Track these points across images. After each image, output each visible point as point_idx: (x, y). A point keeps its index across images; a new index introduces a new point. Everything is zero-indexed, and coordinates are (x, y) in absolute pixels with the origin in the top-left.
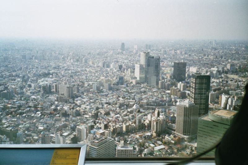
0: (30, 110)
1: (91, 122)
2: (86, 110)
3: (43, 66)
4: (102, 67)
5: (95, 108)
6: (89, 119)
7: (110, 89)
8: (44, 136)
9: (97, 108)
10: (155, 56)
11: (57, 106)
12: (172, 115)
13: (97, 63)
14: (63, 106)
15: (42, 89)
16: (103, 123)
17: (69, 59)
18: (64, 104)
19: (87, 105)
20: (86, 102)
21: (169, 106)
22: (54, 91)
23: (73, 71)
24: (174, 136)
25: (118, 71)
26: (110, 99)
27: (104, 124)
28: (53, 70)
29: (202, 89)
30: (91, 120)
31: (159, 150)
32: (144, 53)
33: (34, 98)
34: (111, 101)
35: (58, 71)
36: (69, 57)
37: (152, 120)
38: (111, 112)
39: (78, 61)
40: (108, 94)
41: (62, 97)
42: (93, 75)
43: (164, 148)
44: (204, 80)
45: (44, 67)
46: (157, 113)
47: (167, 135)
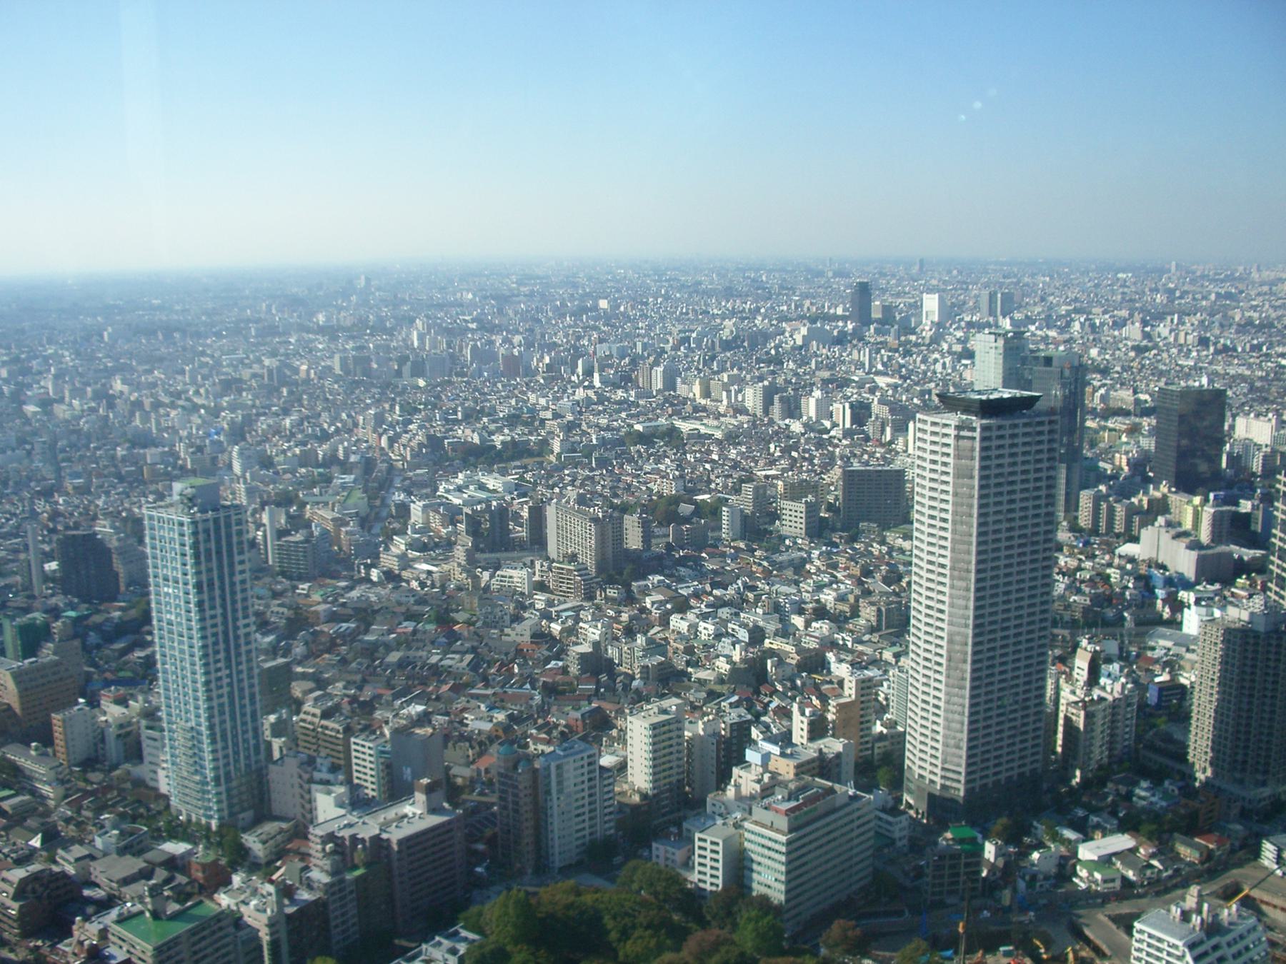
0: (415, 632)
3: (455, 413)
4: (759, 413)
5: (743, 635)
6: (718, 688)
7: (817, 530)
8: (511, 764)
12: (1165, 677)
13: (729, 392)
15: (462, 527)
16: (803, 714)
17: (580, 370)
18: (581, 608)
19: (704, 617)
20: (693, 602)
21: (1142, 629)
23: (608, 435)
24: (1180, 789)
25: (847, 434)
26: (819, 588)
27: (805, 720)
28: (506, 431)
30: (733, 693)
31: (1106, 861)
33: (429, 573)
35: (531, 433)
36: (580, 362)
37: (1062, 701)
38: (831, 656)
39: (625, 380)
40: (804, 561)
43: (1133, 851)
45: (460, 416)
46: (1085, 666)
47: (1144, 784)
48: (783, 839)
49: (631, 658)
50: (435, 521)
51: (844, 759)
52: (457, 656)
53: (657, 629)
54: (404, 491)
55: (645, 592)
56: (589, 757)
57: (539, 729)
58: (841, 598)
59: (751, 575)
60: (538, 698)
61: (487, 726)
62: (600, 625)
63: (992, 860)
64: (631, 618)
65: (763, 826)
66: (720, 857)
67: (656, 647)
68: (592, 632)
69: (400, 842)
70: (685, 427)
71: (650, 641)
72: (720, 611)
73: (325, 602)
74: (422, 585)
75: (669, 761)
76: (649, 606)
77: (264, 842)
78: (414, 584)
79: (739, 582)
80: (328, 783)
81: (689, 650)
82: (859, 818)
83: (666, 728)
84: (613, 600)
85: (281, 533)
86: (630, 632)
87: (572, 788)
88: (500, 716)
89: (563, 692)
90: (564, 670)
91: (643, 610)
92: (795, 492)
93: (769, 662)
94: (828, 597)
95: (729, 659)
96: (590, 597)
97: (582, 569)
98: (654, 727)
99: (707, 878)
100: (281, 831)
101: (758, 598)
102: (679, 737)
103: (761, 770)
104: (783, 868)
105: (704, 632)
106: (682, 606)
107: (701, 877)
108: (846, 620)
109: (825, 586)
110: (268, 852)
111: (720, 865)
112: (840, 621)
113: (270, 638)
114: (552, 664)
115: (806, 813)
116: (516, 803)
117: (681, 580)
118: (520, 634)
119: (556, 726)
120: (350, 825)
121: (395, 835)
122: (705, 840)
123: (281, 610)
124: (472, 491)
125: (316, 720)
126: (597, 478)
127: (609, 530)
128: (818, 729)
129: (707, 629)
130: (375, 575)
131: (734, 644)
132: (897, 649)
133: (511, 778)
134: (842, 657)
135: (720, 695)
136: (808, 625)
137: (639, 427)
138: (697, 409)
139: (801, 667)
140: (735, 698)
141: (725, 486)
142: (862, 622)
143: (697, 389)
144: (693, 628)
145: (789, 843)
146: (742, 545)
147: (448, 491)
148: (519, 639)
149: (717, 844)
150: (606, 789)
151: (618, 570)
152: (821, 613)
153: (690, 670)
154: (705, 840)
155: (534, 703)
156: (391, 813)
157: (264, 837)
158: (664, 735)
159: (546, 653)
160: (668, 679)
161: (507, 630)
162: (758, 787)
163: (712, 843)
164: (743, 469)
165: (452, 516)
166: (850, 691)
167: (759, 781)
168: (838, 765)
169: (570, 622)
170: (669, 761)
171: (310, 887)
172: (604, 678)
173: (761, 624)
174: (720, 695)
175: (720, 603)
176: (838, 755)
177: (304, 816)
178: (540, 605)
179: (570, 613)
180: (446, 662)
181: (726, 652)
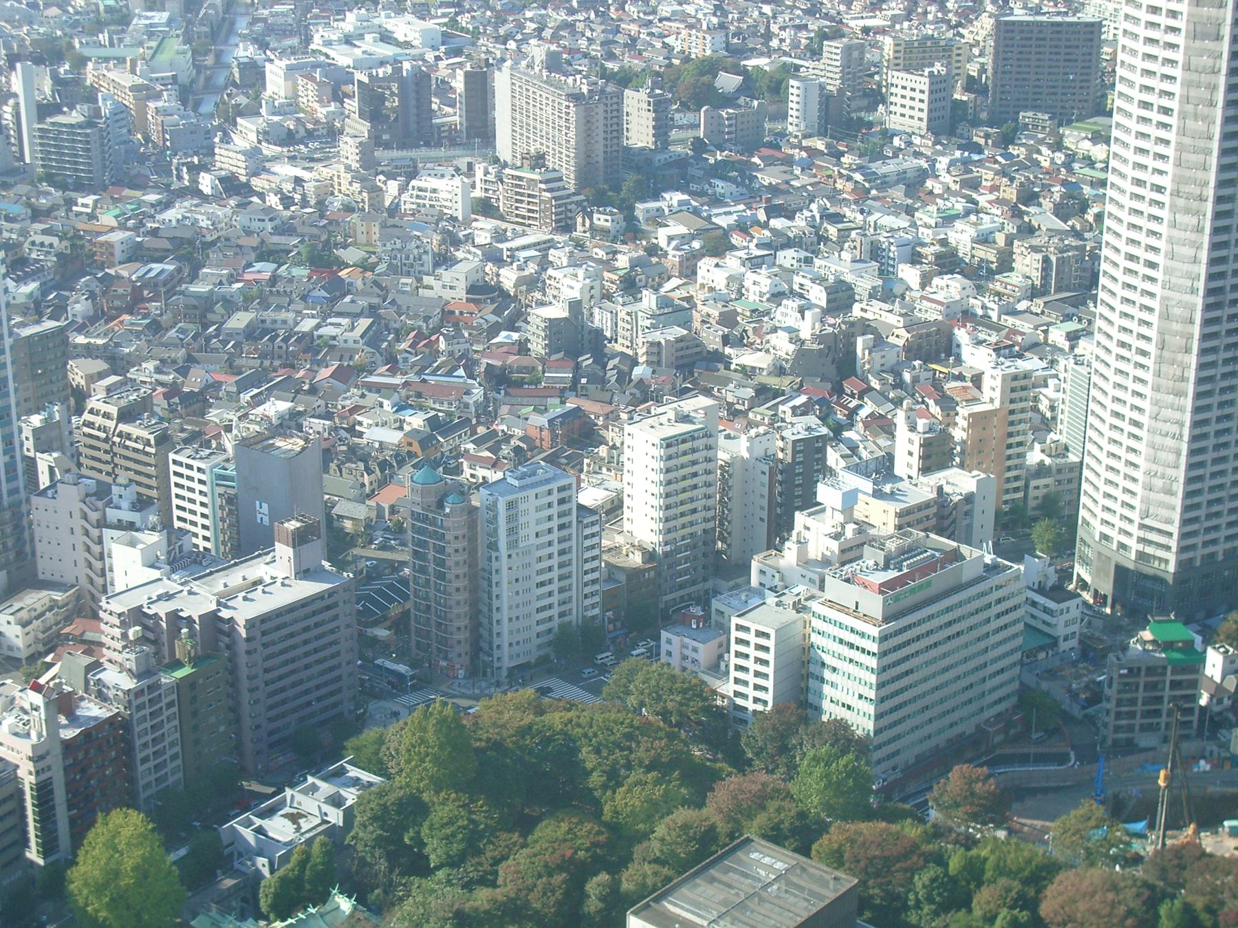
0: (274, 280)
5: (818, 296)
6: (774, 382)
7: (948, 121)
8: (433, 500)
15: (352, 105)
16: (913, 428)
19: (754, 263)
20: (736, 239)
22: (452, 128)
26: (948, 220)
30: (799, 390)
33: (298, 181)
38: (962, 335)
40: (923, 175)
48: (875, 631)
49: (632, 327)
50: (308, 95)
52: (345, 321)
53: (675, 282)
54: (255, 41)
55: (658, 219)
56: (561, 489)
57: (478, 442)
58: (984, 239)
59: (834, 196)
60: (478, 393)
61: (393, 437)
62: (581, 272)
63: (1218, 679)
64: (634, 264)
65: (843, 609)
66: (770, 657)
67: (674, 312)
68: (568, 285)
69: (250, 624)
71: (664, 302)
72: (780, 254)
73: (123, 227)
74: (287, 201)
75: (692, 500)
76: (663, 243)
77: (24, 624)
78: (273, 200)
79: (814, 206)
80: (131, 526)
81: (728, 319)
82: (999, 601)
83: (688, 445)
84: (604, 232)
85: (44, 110)
86: (630, 286)
87: (533, 540)
88: (416, 421)
89: (519, 384)
90: (522, 348)
91: (653, 250)
92: (914, 56)
93: (860, 341)
94: (962, 237)
95: (795, 338)
96: (565, 226)
97: (553, 181)
98: (669, 443)
99: (750, 691)
100: (53, 605)
101: (844, 235)
102: (709, 460)
103: (840, 518)
104: (873, 679)
105: (753, 288)
106: (718, 246)
107: (740, 688)
108: (991, 274)
109: (957, 217)
110: (31, 637)
111: (770, 670)
112: (979, 275)
113: (32, 286)
114: (502, 337)
115: (913, 591)
116: (441, 563)
117: (717, 201)
118: (449, 285)
119: (507, 438)
120: (168, 597)
121: (242, 613)
122: (747, 629)
123: (48, 240)
124: (369, 44)
125: (111, 424)
126: (580, 26)
127: (599, 114)
128: (936, 454)
129: (759, 284)
130: (206, 183)
131: (802, 311)
132: (1073, 326)
133: (433, 522)
134: (982, 336)
135: (777, 393)
136: (925, 281)
139: (912, 351)
140: (802, 399)
141: (795, 44)
142: (1015, 278)
144: (736, 282)
145: (884, 638)
146: (820, 145)
147: (328, 43)
148: (447, 295)
149: (767, 636)
150: (588, 543)
151: (614, 181)
152: (948, 262)
153: (728, 350)
154: (747, 629)
155: (471, 400)
156: (235, 577)
157: (24, 615)
158: (684, 454)
159: (493, 318)
160: (692, 365)
161: (427, 280)
162: (835, 546)
163: (760, 634)
164: (826, 16)
165: (336, 85)
166: (992, 395)
167: (837, 536)
169: (532, 268)
170: (692, 500)
171: (102, 697)
172: (586, 360)
173: (849, 278)
174: (777, 393)
175: (784, 242)
176: (969, 498)
177: (91, 582)
178: (483, 238)
179: (532, 253)
180: (327, 331)
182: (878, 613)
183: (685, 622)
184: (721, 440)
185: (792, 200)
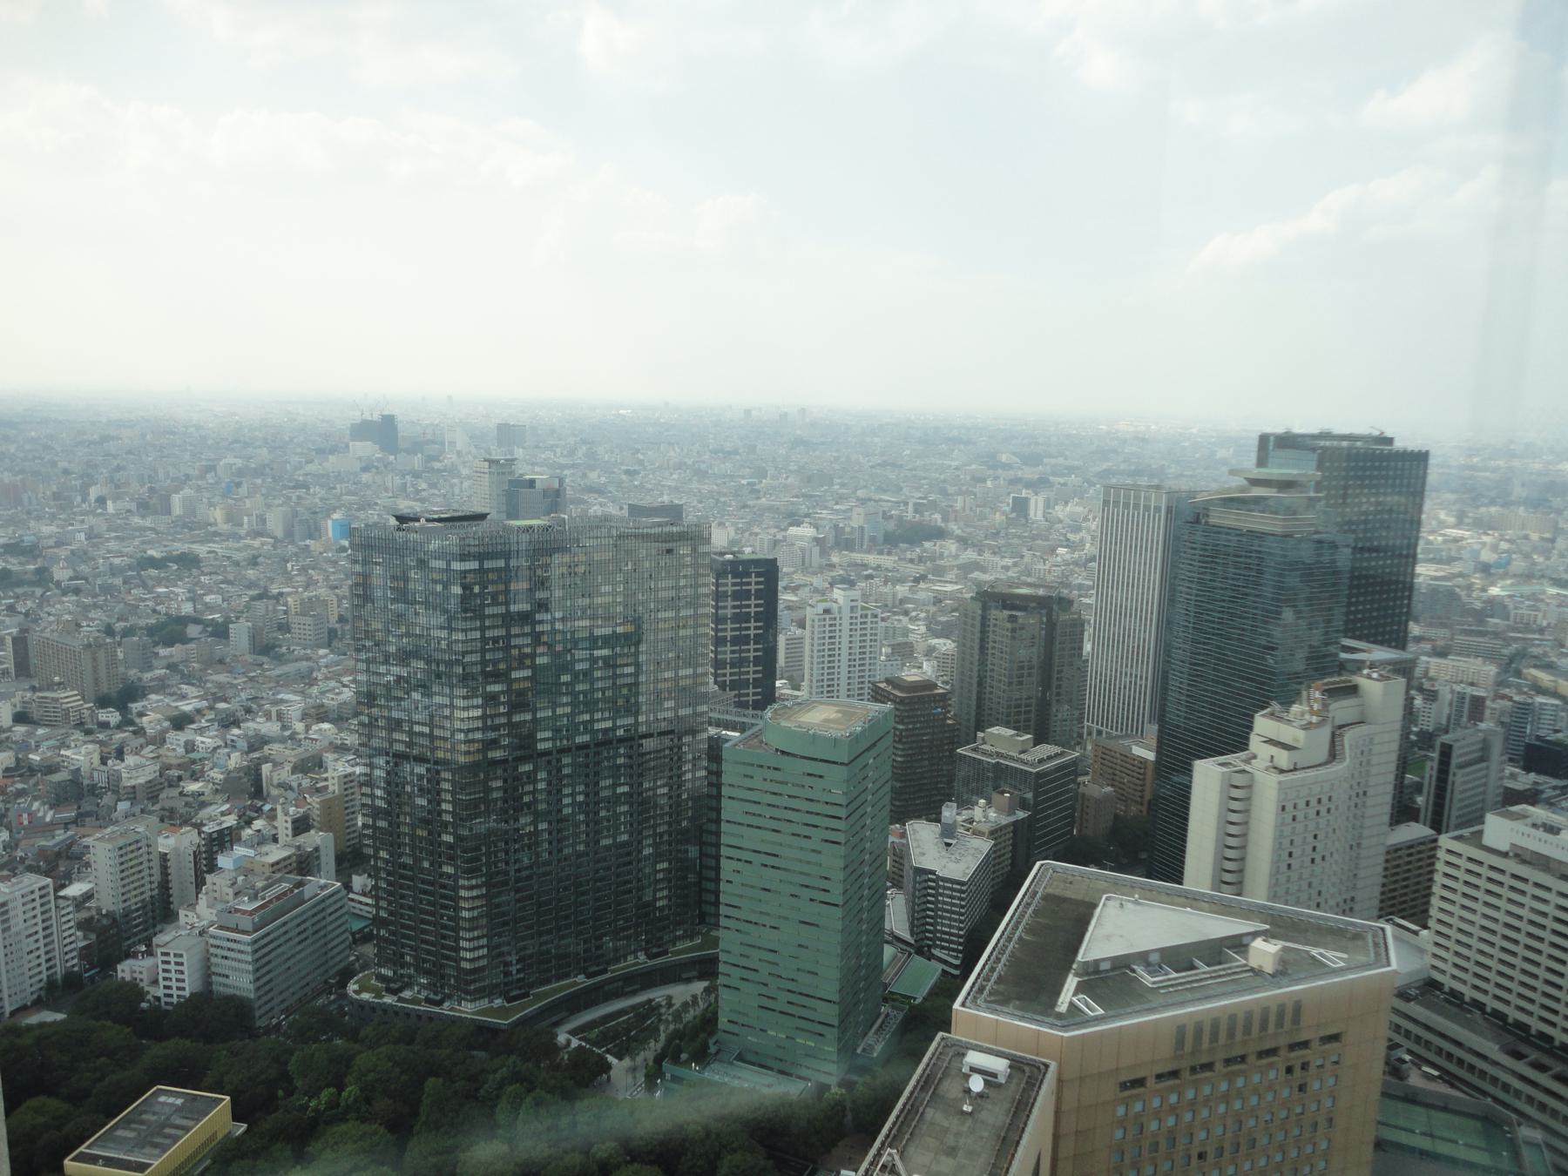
1: (223, 814)
2: (193, 756)
5: (242, 744)
9: (258, 743)
10: (541, 476)
11: (24, 747)
14: (64, 745)
16: (286, 814)
23: (117, 561)
26: (323, 693)
29: (746, 618)
32: (491, 462)
34: (330, 701)
38: (329, 757)
40: (312, 670)
41: (57, 700)
42: (231, 577)
44: (753, 579)
51: (323, 853)
65: (228, 929)
70: (201, 550)
99: (175, 992)
117: (183, 697)
122: (167, 954)
128: (301, 825)
136: (308, 728)
137: (152, 552)
138: (216, 534)
140: (226, 807)
143: (218, 514)
158: (128, 853)
166: (334, 787)
168: (318, 858)
176: (317, 849)
181: (222, 762)
182: (250, 927)
183: (135, 956)
184: (161, 840)
185: (230, 693)
